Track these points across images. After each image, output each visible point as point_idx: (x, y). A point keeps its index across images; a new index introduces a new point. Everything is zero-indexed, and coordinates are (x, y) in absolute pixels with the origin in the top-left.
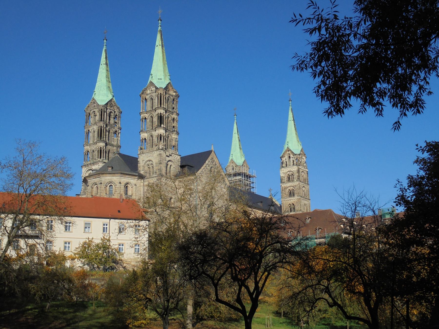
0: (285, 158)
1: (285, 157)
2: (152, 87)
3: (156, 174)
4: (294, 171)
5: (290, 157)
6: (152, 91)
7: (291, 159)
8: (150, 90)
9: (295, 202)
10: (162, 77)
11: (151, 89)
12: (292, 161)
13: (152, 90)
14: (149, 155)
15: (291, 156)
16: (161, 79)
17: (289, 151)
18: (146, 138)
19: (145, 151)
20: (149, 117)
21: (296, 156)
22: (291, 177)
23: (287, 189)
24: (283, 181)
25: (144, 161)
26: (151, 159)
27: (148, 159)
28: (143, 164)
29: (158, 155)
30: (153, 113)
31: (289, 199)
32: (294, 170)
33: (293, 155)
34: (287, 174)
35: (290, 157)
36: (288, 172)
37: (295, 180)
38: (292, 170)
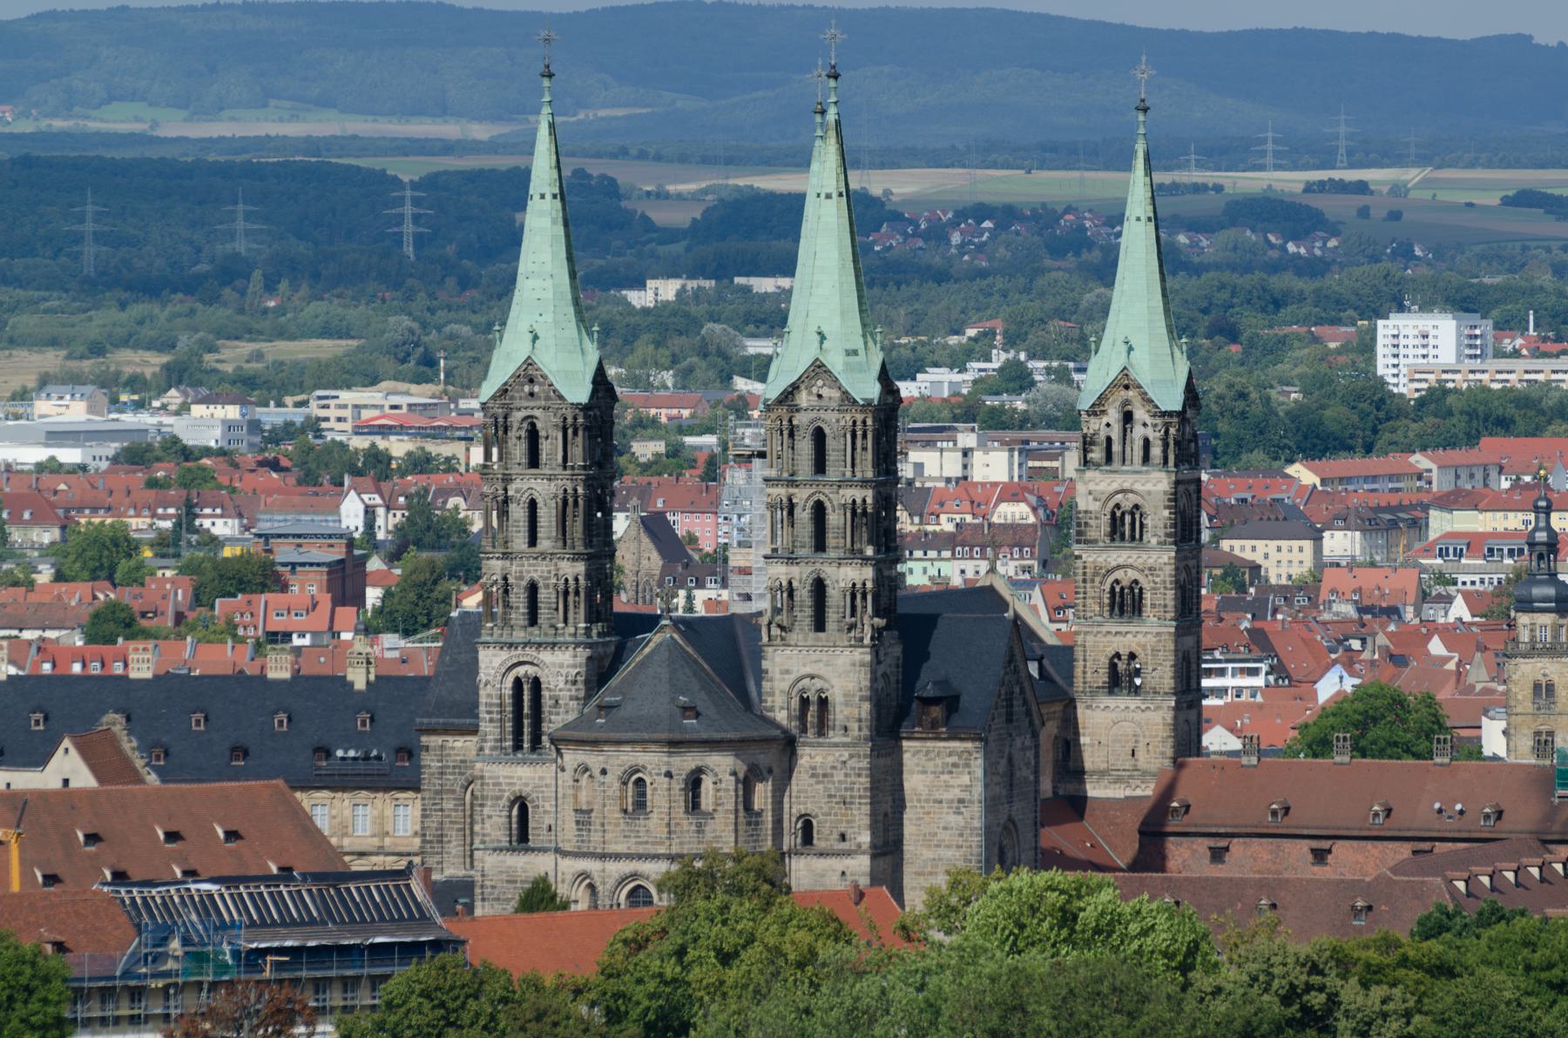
0: (1105, 420)
1: (1103, 412)
2: (820, 383)
3: (847, 736)
4: (1149, 493)
5: (1128, 417)
6: (823, 403)
7: (1138, 432)
8: (810, 393)
9: (1144, 647)
10: (859, 344)
11: (815, 390)
12: (1142, 443)
13: (820, 396)
14: (814, 656)
15: (1140, 414)
16: (855, 353)
17: (1127, 387)
18: (795, 584)
19: (793, 637)
20: (811, 503)
21: (1167, 419)
22: (1128, 518)
23: (1110, 579)
24: (1092, 534)
25: (787, 672)
26: (821, 673)
27: (808, 670)
28: (785, 686)
29: (854, 665)
30: (827, 491)
31: (1114, 630)
32: (1149, 487)
33: (1154, 416)
34: (1111, 504)
35: (1128, 417)
36: (1117, 492)
37: (1154, 541)
38: (1138, 487)
